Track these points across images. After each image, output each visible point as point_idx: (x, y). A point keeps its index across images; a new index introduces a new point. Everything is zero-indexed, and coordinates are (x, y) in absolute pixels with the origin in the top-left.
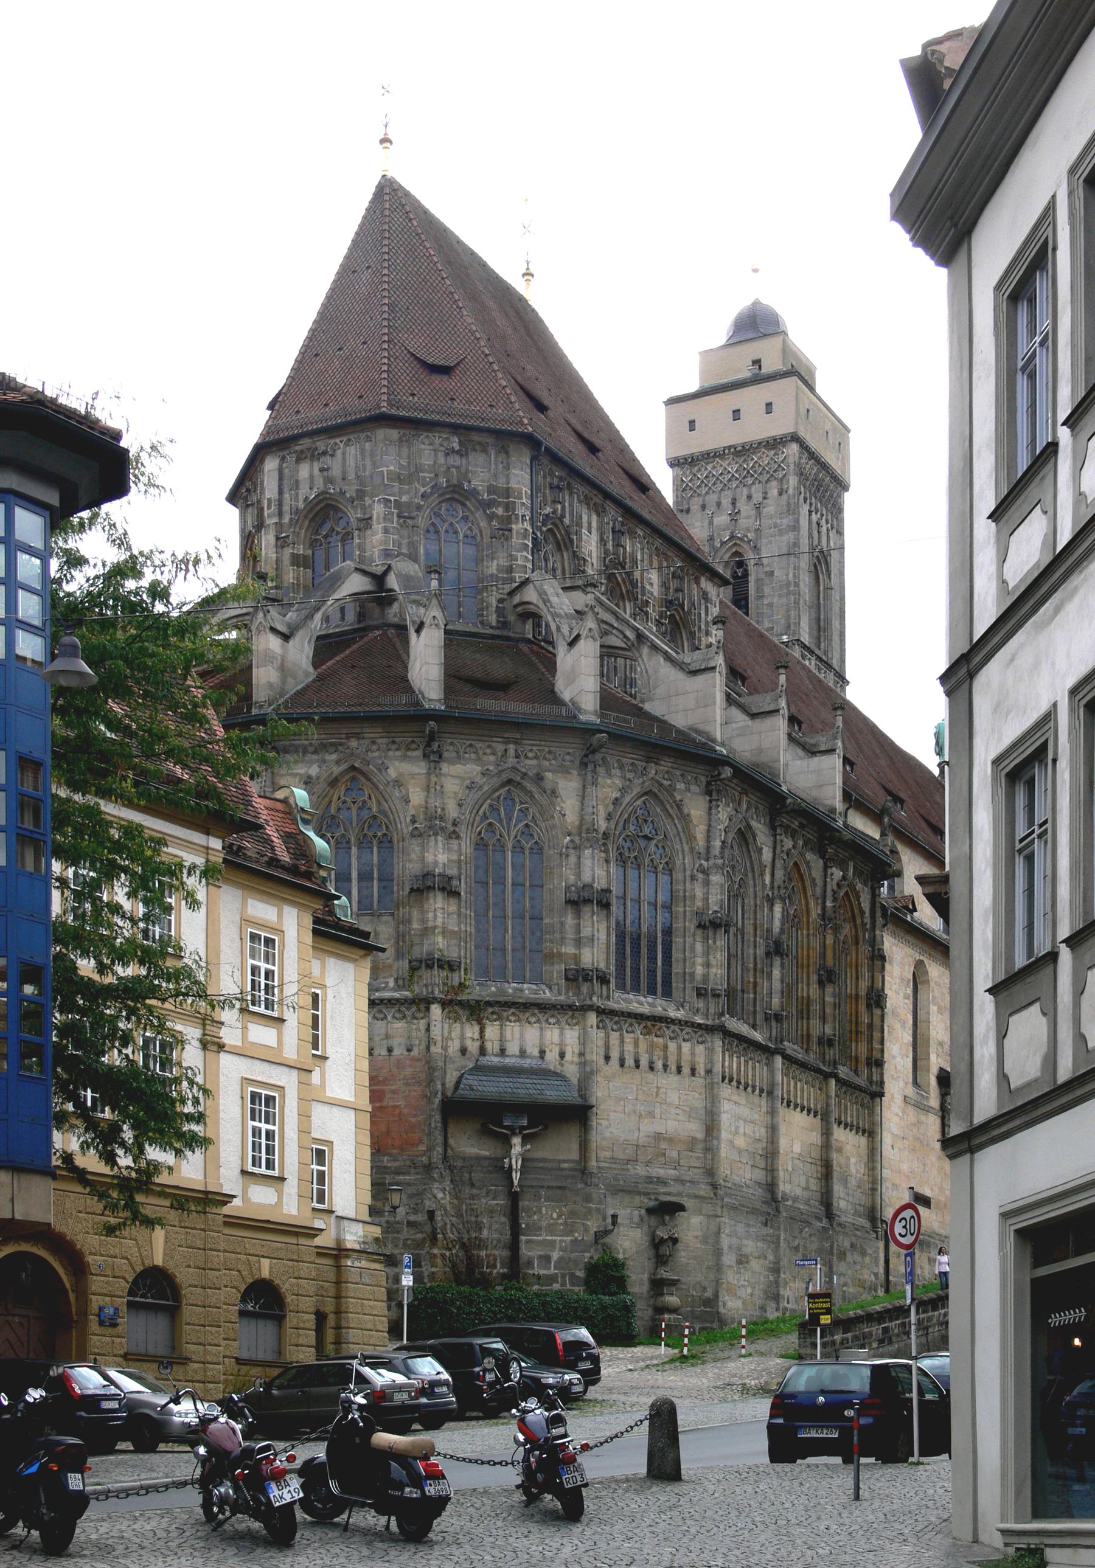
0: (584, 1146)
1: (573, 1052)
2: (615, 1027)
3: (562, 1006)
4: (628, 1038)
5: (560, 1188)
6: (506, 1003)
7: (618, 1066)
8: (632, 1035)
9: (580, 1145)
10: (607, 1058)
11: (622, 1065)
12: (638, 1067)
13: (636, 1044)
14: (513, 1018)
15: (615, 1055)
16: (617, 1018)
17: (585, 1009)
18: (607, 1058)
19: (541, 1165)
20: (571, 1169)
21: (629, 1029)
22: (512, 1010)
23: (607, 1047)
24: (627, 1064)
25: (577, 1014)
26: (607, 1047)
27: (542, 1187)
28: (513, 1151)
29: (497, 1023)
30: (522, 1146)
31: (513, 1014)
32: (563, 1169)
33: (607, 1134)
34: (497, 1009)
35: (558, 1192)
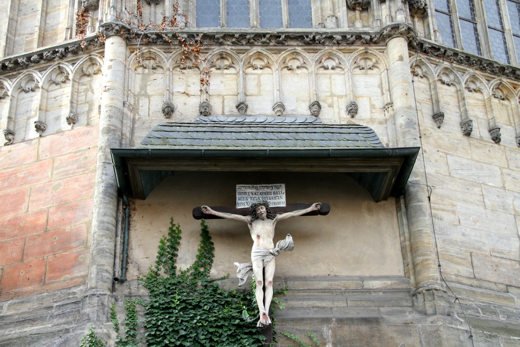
0: (410, 250)
1: (373, 106)
2: (445, 79)
3: (344, 37)
4: (472, 100)
5: (366, 321)
6: (243, 36)
7: (459, 134)
8: (477, 95)
9: (403, 248)
10: (438, 117)
11: (468, 134)
12: (497, 139)
13: (487, 107)
14: (259, 63)
15: (452, 118)
16: (446, 64)
17: (381, 39)
18: (438, 117)
19: (324, 284)
20: (385, 291)
21: (472, 86)
22: (255, 49)
23: (435, 101)
24: (475, 133)
25: (373, 49)
26: (435, 101)
27: (326, 321)
28: (254, 248)
29: (232, 71)
30: (275, 240)
31: (259, 56)
32: (369, 291)
33: (456, 236)
34: (228, 48)
35: (364, 328)
